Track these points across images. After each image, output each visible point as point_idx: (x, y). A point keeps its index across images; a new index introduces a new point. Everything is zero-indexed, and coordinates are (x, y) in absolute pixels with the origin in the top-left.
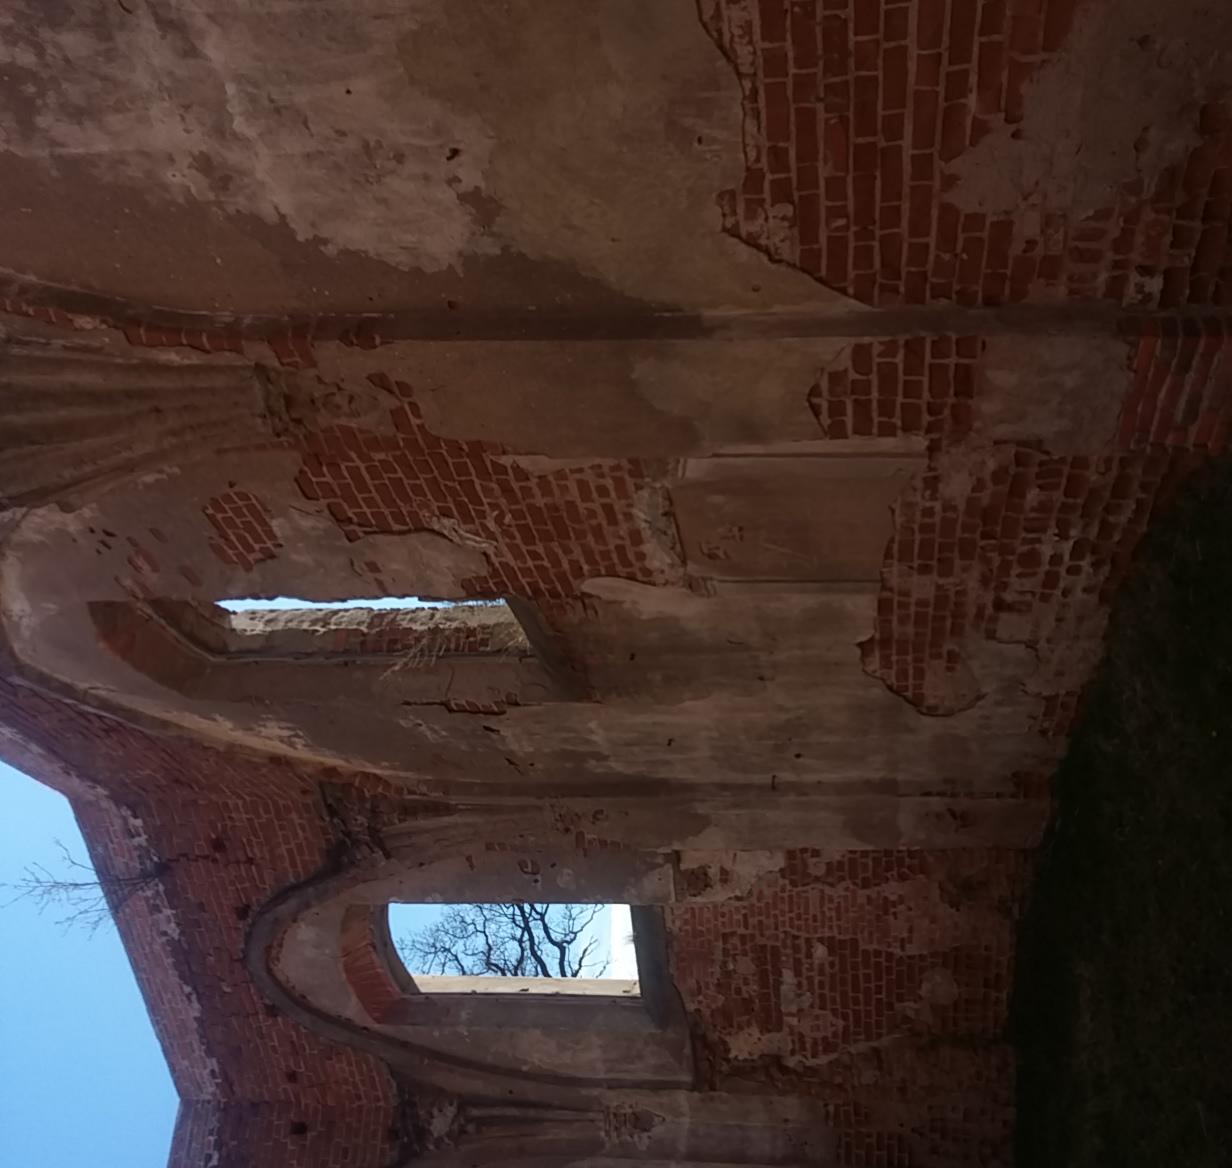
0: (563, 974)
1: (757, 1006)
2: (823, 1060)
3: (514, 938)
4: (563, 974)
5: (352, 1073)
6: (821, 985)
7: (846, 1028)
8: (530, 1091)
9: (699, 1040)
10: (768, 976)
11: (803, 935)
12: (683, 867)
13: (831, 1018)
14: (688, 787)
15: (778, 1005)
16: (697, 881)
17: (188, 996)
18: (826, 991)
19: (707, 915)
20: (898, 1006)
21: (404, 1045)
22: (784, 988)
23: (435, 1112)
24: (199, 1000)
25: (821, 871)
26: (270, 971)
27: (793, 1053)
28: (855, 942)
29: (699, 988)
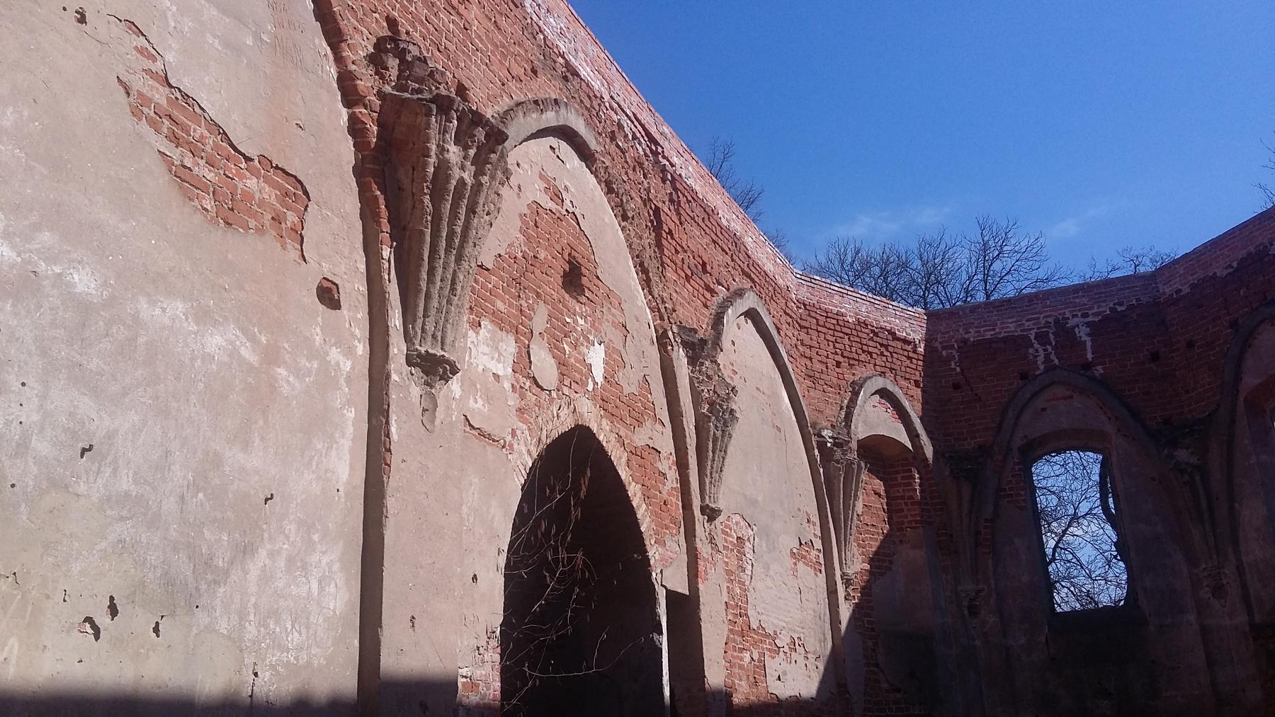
26: (1262, 321)
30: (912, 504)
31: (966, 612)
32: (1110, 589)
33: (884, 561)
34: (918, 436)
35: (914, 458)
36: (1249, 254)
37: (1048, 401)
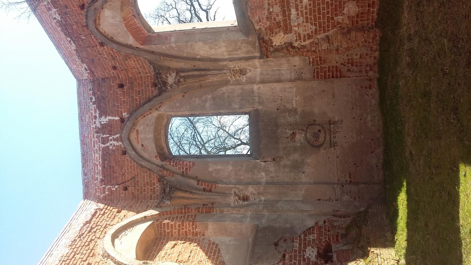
0: (208, 20)
1: (282, 24)
2: (308, 42)
3: (188, 10)
4: (208, 20)
5: (135, 64)
6: (306, 13)
7: (316, 30)
8: (201, 65)
9: (262, 40)
10: (286, 13)
13: (310, 26)
15: (290, 23)
17: (70, 42)
18: (308, 16)
22: (292, 16)
23: (168, 75)
24: (74, 43)
26: (97, 29)
27: (296, 40)
29: (260, 21)
30: (183, 225)
31: (246, 203)
32: (239, 123)
33: (212, 248)
34: (145, 217)
35: (157, 220)
36: (62, 30)
37: (138, 143)
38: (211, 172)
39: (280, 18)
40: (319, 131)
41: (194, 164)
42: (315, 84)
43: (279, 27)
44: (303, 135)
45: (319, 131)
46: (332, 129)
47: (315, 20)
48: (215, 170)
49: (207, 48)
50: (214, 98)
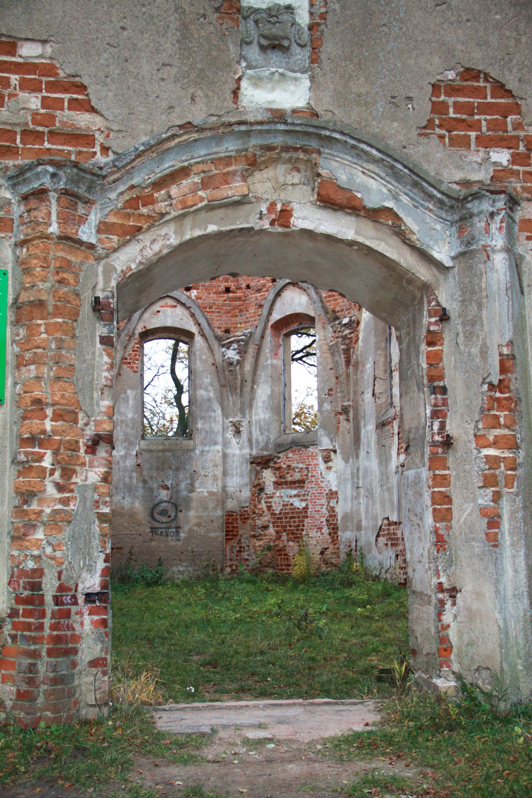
1: (283, 480)
2: (264, 505)
8: (247, 388)
10: (294, 484)
11: (309, 498)
12: (332, 453)
13: (279, 508)
14: (357, 456)
16: (327, 459)
19: (315, 462)
20: (285, 534)
21: (262, 337)
25: (331, 504)
28: (307, 517)
37: (162, 307)
38: (126, 393)
39: (290, 479)
40: (169, 517)
41: (135, 372)
42: (219, 513)
43: (281, 477)
44: (165, 499)
45: (169, 517)
46: (170, 530)
47: (284, 513)
48: (128, 397)
49: (265, 398)
50: (209, 400)
